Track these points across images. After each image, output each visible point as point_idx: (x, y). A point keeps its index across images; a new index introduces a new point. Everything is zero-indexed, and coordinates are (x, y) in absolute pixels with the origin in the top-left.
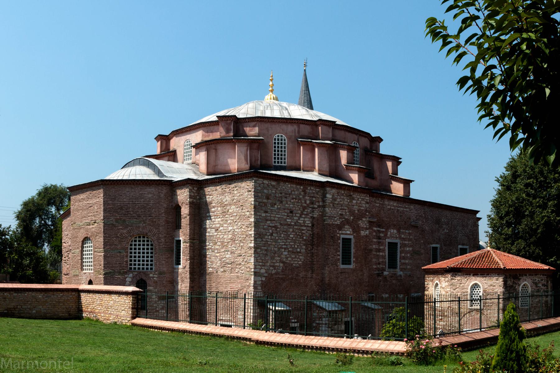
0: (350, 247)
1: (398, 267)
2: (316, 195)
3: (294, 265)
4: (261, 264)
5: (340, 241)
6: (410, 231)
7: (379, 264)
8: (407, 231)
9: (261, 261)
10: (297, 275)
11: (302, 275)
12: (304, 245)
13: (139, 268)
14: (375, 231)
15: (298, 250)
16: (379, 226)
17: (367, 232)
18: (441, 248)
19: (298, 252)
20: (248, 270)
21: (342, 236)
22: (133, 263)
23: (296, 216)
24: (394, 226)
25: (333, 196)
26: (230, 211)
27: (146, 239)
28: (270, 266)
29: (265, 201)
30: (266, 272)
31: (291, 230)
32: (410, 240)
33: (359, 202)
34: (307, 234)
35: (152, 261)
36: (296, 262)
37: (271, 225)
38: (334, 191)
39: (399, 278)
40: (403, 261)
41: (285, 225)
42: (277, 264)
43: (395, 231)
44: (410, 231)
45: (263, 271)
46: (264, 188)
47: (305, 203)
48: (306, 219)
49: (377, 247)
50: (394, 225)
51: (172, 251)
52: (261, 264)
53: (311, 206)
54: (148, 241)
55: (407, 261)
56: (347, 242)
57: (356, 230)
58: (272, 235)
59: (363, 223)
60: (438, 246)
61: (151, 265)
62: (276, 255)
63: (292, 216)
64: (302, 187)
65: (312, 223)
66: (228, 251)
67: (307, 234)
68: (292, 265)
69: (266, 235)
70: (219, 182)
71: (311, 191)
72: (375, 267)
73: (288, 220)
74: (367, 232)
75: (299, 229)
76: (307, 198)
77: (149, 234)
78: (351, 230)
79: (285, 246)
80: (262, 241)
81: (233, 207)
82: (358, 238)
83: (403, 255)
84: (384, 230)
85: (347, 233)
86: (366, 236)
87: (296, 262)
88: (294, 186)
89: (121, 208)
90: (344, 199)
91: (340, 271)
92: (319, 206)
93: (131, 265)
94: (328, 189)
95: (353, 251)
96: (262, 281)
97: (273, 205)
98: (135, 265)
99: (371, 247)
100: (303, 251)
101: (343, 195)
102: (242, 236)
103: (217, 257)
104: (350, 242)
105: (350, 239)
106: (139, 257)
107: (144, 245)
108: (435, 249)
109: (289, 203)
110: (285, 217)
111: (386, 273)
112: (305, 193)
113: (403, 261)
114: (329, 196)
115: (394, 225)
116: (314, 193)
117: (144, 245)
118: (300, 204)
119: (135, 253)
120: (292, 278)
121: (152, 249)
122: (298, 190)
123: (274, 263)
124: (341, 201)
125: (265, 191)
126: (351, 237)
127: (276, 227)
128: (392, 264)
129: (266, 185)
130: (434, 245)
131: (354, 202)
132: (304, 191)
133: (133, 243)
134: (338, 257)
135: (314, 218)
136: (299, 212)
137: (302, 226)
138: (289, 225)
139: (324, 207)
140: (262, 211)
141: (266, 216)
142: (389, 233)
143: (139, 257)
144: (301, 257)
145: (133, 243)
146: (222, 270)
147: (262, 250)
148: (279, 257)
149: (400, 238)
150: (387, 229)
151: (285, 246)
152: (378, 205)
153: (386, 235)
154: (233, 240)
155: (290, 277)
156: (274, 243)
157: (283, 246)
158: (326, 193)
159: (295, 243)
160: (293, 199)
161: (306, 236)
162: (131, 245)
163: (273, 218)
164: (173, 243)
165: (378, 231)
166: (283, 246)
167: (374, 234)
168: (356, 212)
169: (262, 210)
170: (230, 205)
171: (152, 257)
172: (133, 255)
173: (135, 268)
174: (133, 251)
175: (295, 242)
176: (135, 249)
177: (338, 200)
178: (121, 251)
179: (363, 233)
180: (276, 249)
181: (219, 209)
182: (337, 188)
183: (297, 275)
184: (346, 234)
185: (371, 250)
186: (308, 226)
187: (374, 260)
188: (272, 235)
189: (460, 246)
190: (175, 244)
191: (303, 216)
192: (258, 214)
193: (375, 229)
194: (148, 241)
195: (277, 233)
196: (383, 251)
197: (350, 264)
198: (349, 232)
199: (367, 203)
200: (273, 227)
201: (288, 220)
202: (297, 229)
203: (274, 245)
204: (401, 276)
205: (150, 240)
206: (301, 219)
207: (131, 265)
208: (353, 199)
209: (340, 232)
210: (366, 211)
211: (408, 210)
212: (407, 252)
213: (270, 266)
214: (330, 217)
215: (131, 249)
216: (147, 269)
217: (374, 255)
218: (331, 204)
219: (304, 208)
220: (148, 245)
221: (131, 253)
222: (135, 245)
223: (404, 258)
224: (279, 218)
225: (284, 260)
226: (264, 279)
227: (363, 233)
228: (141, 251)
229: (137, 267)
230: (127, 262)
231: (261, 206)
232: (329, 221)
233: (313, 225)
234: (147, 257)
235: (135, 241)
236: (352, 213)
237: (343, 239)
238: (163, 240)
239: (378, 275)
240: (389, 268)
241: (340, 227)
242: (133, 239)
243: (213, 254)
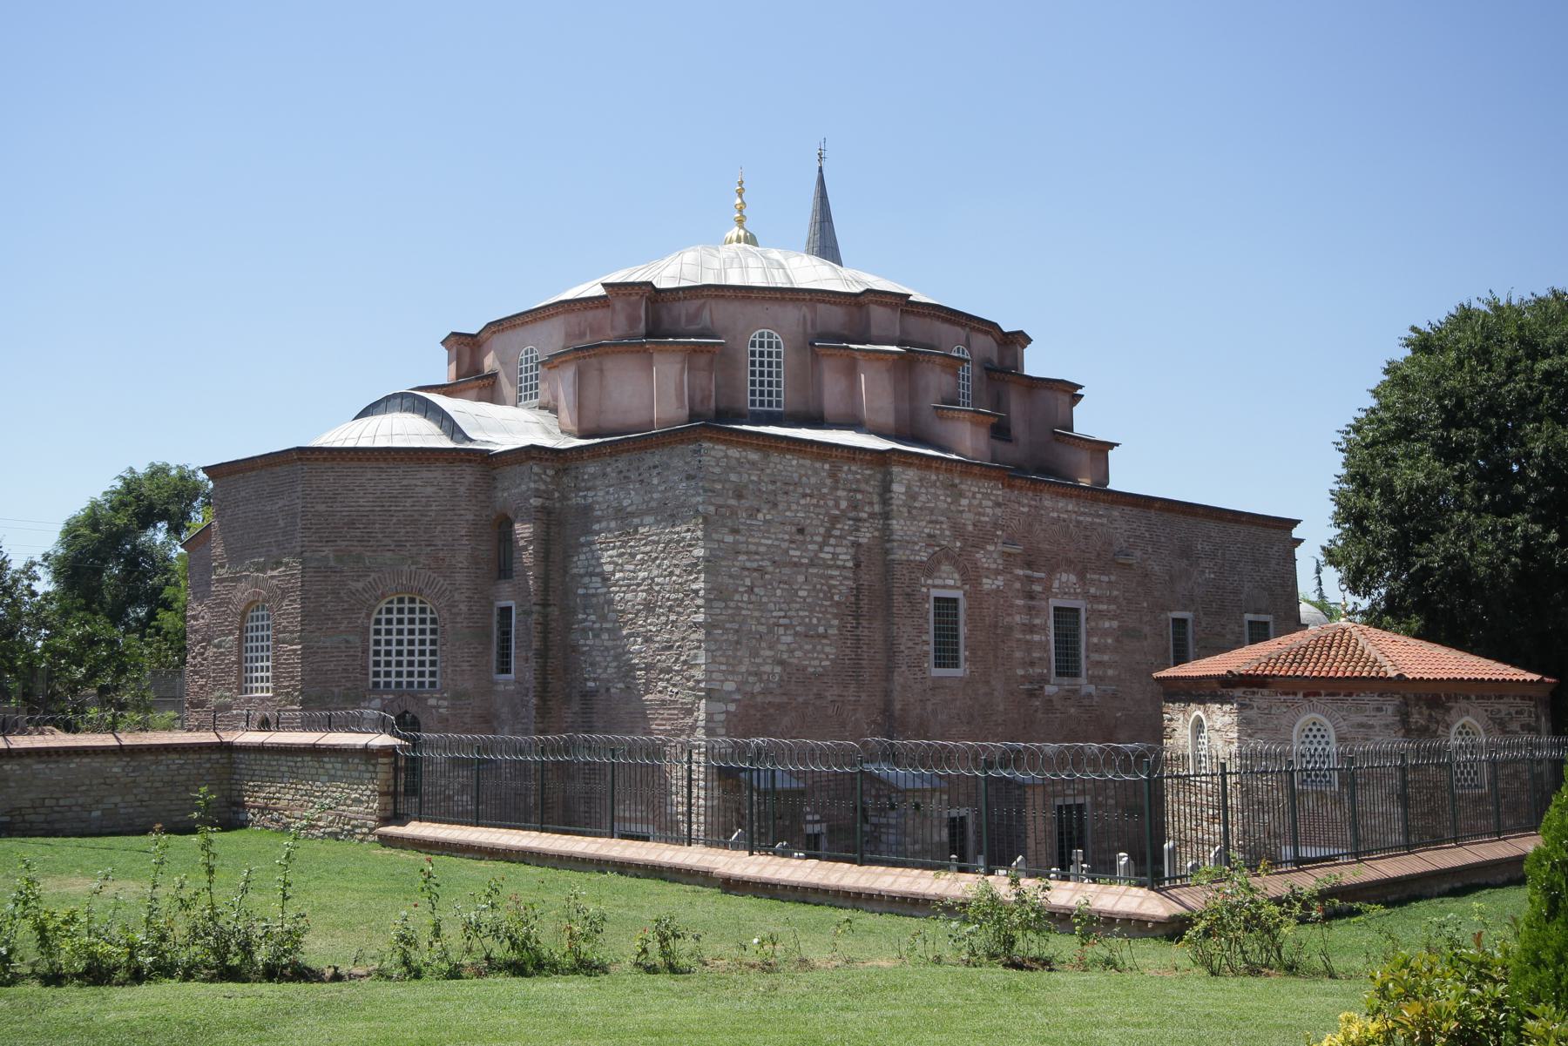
0: (957, 623)
1: (1084, 673)
2: (863, 486)
3: (811, 670)
4: (723, 667)
5: (930, 606)
6: (1113, 578)
7: (1032, 664)
8: (1105, 578)
9: (723, 660)
10: (819, 696)
11: (830, 695)
12: (836, 616)
13: (399, 684)
14: (1018, 578)
15: (821, 630)
16: (1029, 565)
17: (1000, 582)
18: (1197, 622)
19: (819, 636)
20: (691, 684)
21: (935, 593)
22: (382, 669)
23: (812, 542)
24: (1070, 564)
25: (909, 487)
26: (641, 530)
27: (417, 606)
28: (750, 674)
29: (732, 502)
30: (738, 690)
31: (801, 578)
32: (1112, 600)
33: (976, 502)
34: (842, 586)
35: (433, 663)
36: (816, 663)
37: (748, 564)
38: (911, 474)
39: (1086, 702)
40: (1096, 657)
41: (785, 565)
42: (767, 668)
43: (1073, 578)
44: (1113, 578)
45: (730, 686)
46: (731, 469)
47: (837, 506)
48: (839, 550)
49: (1025, 619)
50: (1069, 562)
51: (489, 636)
52: (723, 667)
53: (852, 514)
54: (423, 611)
55: (1106, 658)
56: (946, 607)
57: (970, 575)
58: (751, 590)
59: (989, 557)
61: (433, 674)
62: (764, 645)
63: (804, 542)
64: (827, 466)
65: (855, 558)
66: (638, 635)
67: (844, 589)
68: (805, 668)
69: (736, 591)
70: (611, 455)
71: (850, 477)
72: (1020, 672)
73: (792, 553)
74: (1000, 582)
75: (822, 576)
76: (840, 493)
77: (427, 591)
78: (956, 576)
79: (786, 621)
80: (727, 607)
82: (975, 596)
83: (1095, 640)
84: (1042, 575)
85: (947, 584)
86: (998, 590)
87: (816, 663)
88: (808, 462)
89: (351, 524)
90: (936, 497)
91: (929, 683)
92: (872, 515)
93: (377, 674)
94: (896, 469)
95: (963, 630)
96: (727, 712)
98: (388, 674)
99: (1008, 619)
101: (934, 485)
102: (673, 596)
103: (607, 649)
104: (956, 608)
105: (955, 600)
106: (400, 653)
107: (412, 621)
108: (1180, 624)
109: (794, 507)
110: (785, 545)
111: (1050, 689)
112: (837, 481)
113: (1096, 657)
114: (898, 488)
115: (1069, 562)
116: (858, 481)
117: (412, 621)
118: (822, 511)
119: (388, 643)
120: (806, 703)
121: (433, 632)
122: (816, 472)
123: (759, 665)
124: (929, 501)
125: (733, 477)
126: (958, 594)
128: (1067, 664)
129: (734, 462)
131: (964, 502)
132: (833, 475)
133: (384, 616)
134: (926, 648)
135: (859, 545)
136: (822, 530)
137: (830, 567)
138: (795, 564)
139: (886, 516)
140: (726, 530)
141: (736, 542)
142: (1056, 584)
143: (400, 653)
144: (827, 649)
145: (384, 616)
146: (621, 685)
147: (726, 631)
148: (770, 648)
150: (1052, 570)
151: (786, 621)
152: (1025, 510)
153: (1048, 589)
154: (649, 608)
155: (800, 699)
156: (757, 614)
157: (782, 621)
158: (891, 481)
159: (812, 611)
160: (804, 496)
161: (840, 593)
162: (378, 622)
163: (752, 548)
164: (491, 615)
165: (1027, 577)
166: (782, 621)
167: (1018, 585)
168: (970, 528)
169: (724, 526)
170: (642, 514)
171: (433, 653)
172: (383, 648)
173: (388, 684)
174: (383, 637)
175: (811, 609)
176: (389, 632)
177: (923, 498)
178: (351, 638)
179: (987, 584)
180: (763, 629)
181: (613, 524)
182: (919, 467)
183: (819, 696)
184: (944, 587)
185: (1010, 628)
187: (1018, 654)
188: (751, 590)
189: (1249, 617)
190: (495, 618)
191: (832, 541)
192: (715, 536)
193: (1020, 572)
194: (423, 611)
195: (764, 586)
196: (1044, 628)
197: (957, 666)
198: (951, 582)
199: (998, 505)
200: (755, 570)
201: (792, 553)
202: (816, 575)
203: (758, 619)
204: (1089, 696)
205: (428, 606)
206: (827, 549)
207: (377, 674)
208: (961, 495)
209: (930, 582)
210: (996, 525)
211: (1105, 521)
212: (1106, 633)
213: (750, 674)
214: (906, 543)
215: (378, 632)
216: (421, 684)
217: (1018, 640)
218: (905, 510)
219: (834, 520)
220: (423, 621)
221: (377, 643)
222: (389, 622)
223: (1098, 649)
224: (769, 546)
225: (785, 656)
226: (732, 707)
227: (987, 584)
228: (406, 637)
229: (393, 679)
230: (366, 668)
231: (723, 516)
232: (899, 555)
233: (857, 565)
234: (422, 653)
235: (389, 611)
236: (958, 531)
238: (463, 607)
239: (1031, 694)
240: (1058, 674)
241: (930, 569)
242: (383, 605)
243: (598, 642)
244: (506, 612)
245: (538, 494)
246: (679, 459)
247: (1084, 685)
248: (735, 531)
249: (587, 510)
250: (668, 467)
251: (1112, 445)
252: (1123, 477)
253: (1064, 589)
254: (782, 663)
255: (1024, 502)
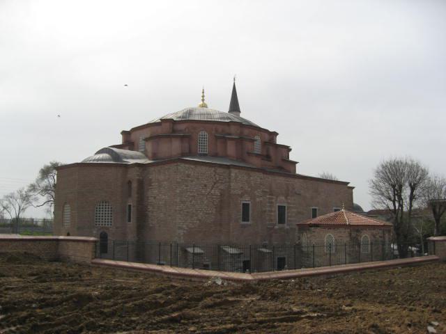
5: (241, 206)
12: (216, 208)
17: (261, 199)
21: (242, 202)
25: (236, 174)
38: (237, 171)
43: (283, 198)
58: (191, 202)
60: (317, 208)
65: (221, 193)
81: (165, 183)
85: (246, 200)
86: (261, 202)
88: (207, 168)
95: (250, 212)
97: (192, 181)
100: (214, 212)
111: (276, 227)
114: (233, 175)
126: (250, 202)
127: (194, 196)
128: (281, 220)
130: (314, 207)
132: (214, 171)
139: (229, 182)
149: (288, 203)
150: (277, 197)
153: (276, 201)
179: (258, 200)
185: (265, 211)
186: (217, 196)
187: (267, 218)
196: (275, 211)
197: (248, 220)
226: (185, 231)
227: (258, 200)
232: (232, 192)
237: (243, 204)
241: (241, 196)
244: (130, 206)
245: (138, 175)
246: (173, 167)
247: (286, 226)
248: (187, 186)
249: (151, 179)
250: (169, 169)
251: (296, 163)
252: (300, 170)
253: (281, 201)
254: (200, 220)
255: (270, 178)
